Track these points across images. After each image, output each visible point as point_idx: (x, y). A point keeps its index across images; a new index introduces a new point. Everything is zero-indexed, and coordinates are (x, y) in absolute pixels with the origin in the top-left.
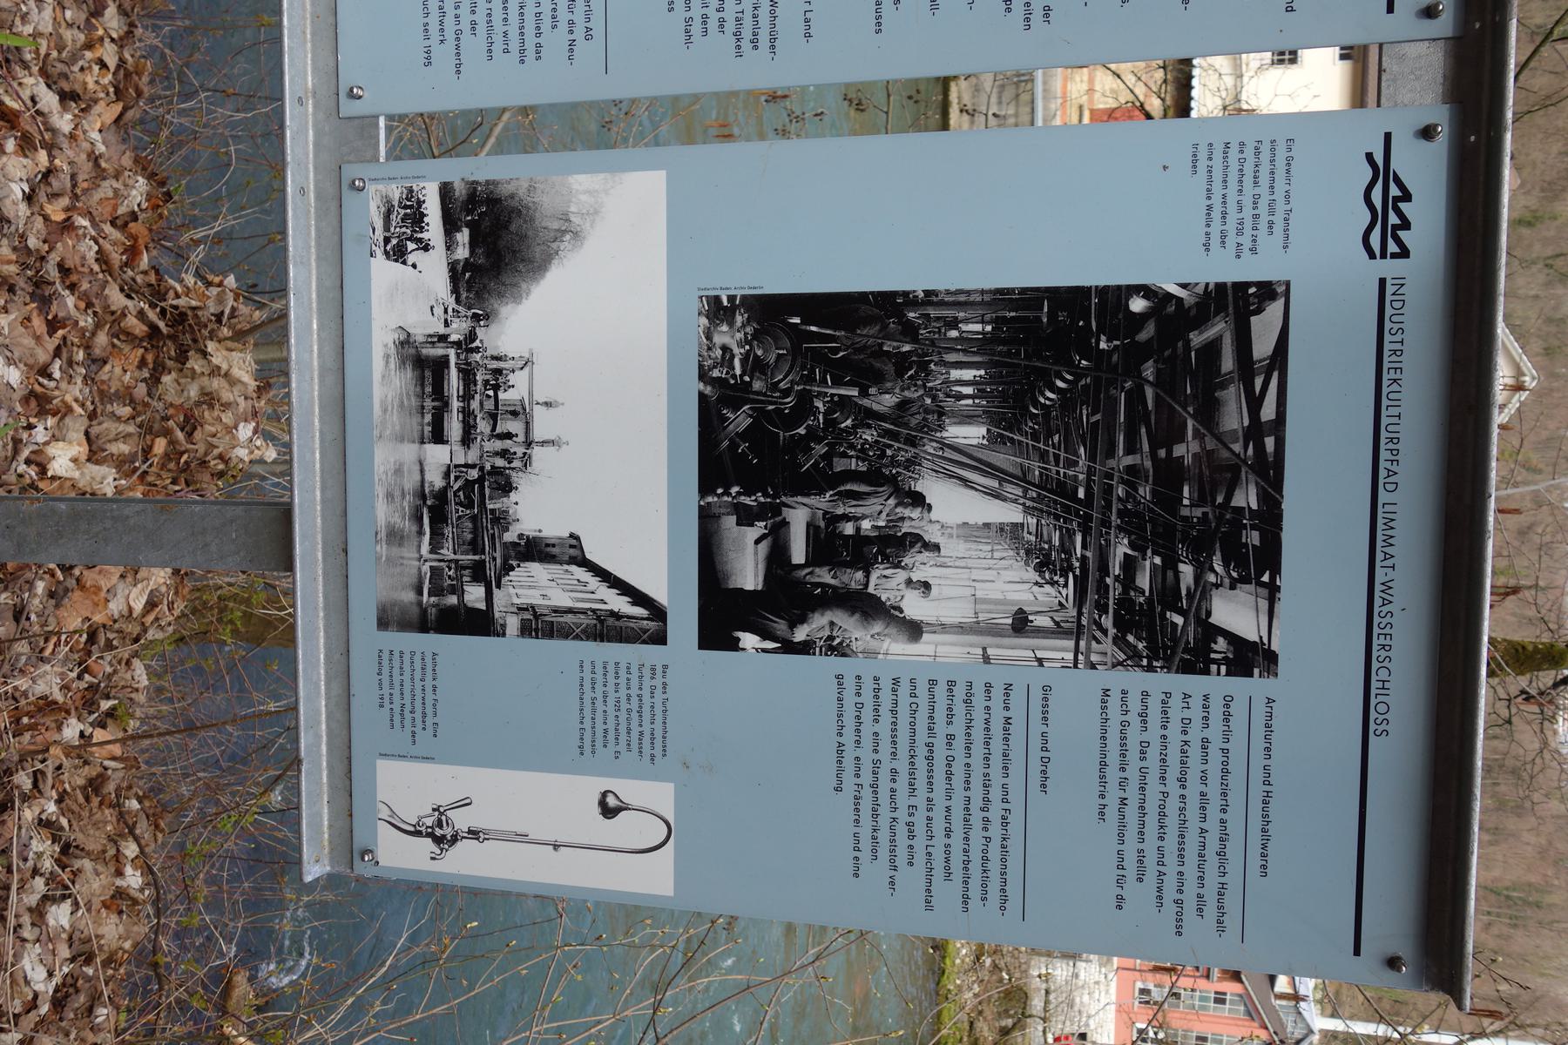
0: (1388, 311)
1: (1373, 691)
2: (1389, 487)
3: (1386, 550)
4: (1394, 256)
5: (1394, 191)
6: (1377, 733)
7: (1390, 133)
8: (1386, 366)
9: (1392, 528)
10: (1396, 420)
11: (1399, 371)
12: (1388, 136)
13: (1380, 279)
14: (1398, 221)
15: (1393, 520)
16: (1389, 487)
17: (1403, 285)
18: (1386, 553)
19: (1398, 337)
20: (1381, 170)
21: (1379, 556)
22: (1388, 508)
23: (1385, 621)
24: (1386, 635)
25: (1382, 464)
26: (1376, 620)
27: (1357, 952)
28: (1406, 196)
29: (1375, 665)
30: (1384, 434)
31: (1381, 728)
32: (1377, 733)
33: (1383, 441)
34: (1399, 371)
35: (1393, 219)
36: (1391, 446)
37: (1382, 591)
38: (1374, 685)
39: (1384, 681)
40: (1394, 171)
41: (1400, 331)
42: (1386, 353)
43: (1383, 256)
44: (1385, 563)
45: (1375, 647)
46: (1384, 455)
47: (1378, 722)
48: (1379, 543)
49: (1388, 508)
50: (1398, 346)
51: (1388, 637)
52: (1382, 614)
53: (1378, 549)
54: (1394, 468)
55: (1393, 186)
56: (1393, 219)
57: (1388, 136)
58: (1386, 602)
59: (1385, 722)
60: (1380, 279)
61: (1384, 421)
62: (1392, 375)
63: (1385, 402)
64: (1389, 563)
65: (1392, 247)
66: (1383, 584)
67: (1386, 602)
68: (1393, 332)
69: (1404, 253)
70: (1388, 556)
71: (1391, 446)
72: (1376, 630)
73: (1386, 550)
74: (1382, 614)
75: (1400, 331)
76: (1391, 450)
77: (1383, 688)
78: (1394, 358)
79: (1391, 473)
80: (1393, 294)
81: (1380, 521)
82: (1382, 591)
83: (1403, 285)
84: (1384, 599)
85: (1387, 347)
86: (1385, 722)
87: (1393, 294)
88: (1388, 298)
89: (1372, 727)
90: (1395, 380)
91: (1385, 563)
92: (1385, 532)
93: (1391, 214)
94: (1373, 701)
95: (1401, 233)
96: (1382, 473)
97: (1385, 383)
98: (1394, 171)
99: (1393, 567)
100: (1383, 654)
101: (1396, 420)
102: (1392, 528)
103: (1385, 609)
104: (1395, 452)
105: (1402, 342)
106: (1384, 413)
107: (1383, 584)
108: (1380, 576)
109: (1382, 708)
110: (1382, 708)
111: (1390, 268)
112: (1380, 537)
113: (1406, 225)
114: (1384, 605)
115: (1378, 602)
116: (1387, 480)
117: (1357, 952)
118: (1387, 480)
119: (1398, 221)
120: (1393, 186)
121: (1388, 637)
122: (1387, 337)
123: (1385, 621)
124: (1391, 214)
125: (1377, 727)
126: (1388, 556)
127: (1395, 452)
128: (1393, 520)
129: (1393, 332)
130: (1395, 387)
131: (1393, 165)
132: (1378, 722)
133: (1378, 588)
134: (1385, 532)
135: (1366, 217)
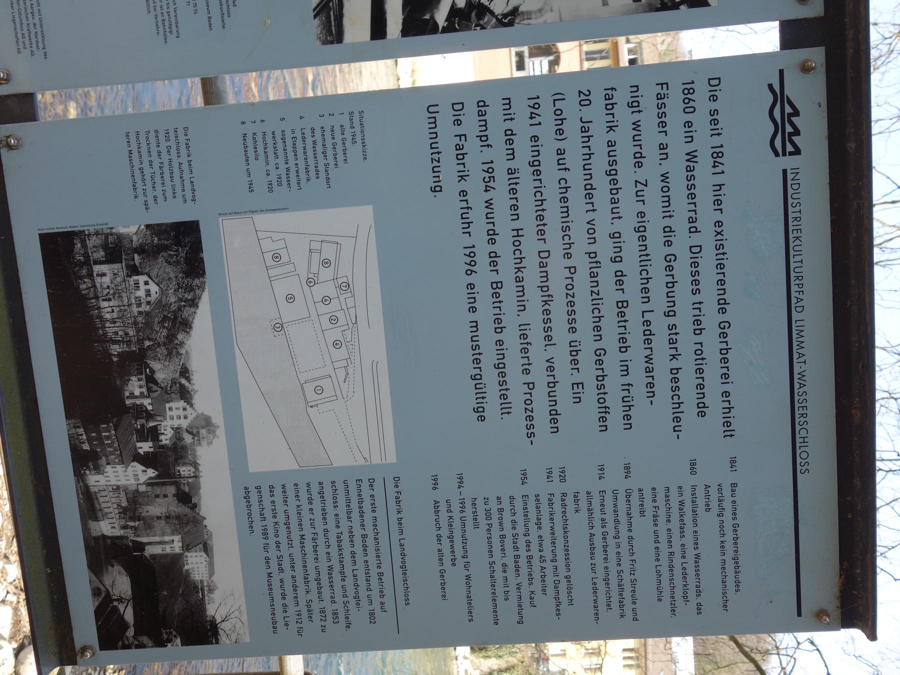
0: (790, 191)
1: (798, 445)
2: (799, 309)
3: (800, 351)
4: (791, 154)
5: (788, 110)
6: (802, 472)
7: (783, 70)
8: (791, 228)
9: (802, 336)
10: (799, 264)
11: (799, 231)
12: (781, 72)
13: (783, 170)
14: (791, 130)
15: (802, 331)
16: (799, 309)
17: (798, 173)
18: (799, 354)
19: (797, 209)
20: (779, 96)
21: (795, 356)
22: (799, 323)
23: (802, 398)
24: (803, 407)
25: (793, 294)
26: (796, 398)
27: (799, 614)
28: (796, 113)
29: (798, 428)
30: (793, 274)
31: (804, 468)
32: (802, 472)
33: (792, 279)
34: (799, 231)
35: (789, 129)
36: (798, 282)
37: (799, 379)
38: (798, 440)
39: (804, 438)
40: (787, 96)
41: (798, 204)
42: (790, 220)
43: (784, 154)
44: (800, 360)
45: (797, 416)
46: (794, 288)
47: (802, 464)
48: (795, 347)
49: (799, 323)
50: (798, 215)
51: (805, 408)
52: (800, 394)
53: (795, 351)
54: (801, 296)
55: (787, 106)
56: (789, 129)
57: (781, 72)
58: (802, 386)
59: (807, 464)
60: (783, 170)
61: (792, 265)
62: (795, 235)
63: (792, 253)
64: (802, 360)
65: (790, 148)
66: (799, 374)
67: (802, 386)
68: (794, 205)
69: (797, 151)
70: (801, 355)
71: (798, 282)
72: (797, 405)
73: (798, 351)
74: (800, 394)
75: (798, 204)
76: (798, 285)
77: (804, 442)
78: (796, 223)
79: (799, 300)
80: (792, 180)
81: (794, 332)
82: (799, 379)
83: (798, 173)
84: (800, 384)
85: (791, 215)
86: (807, 464)
87: (792, 180)
88: (789, 182)
89: (799, 468)
90: (797, 238)
91: (800, 360)
92: (798, 340)
93: (787, 124)
94: (798, 452)
95: (794, 138)
96: (794, 300)
97: (791, 240)
98: (787, 97)
99: (805, 362)
100: (802, 419)
101: (799, 264)
102: (802, 336)
103: (802, 390)
104: (800, 286)
105: (800, 212)
106: (792, 260)
107: (799, 374)
108: (797, 370)
109: (804, 455)
110: (804, 455)
111: (788, 162)
112: (795, 344)
113: (797, 132)
114: (800, 387)
115: (796, 386)
116: (797, 305)
117: (799, 614)
118: (797, 305)
119: (791, 130)
120: (787, 106)
121: (805, 408)
122: (790, 209)
123: (802, 398)
124: (787, 124)
125: (802, 468)
126: (801, 355)
127: (800, 286)
128: (802, 331)
129: (794, 205)
130: (797, 242)
131: (786, 92)
132: (802, 464)
133: (796, 376)
134: (798, 340)
135: (771, 128)
